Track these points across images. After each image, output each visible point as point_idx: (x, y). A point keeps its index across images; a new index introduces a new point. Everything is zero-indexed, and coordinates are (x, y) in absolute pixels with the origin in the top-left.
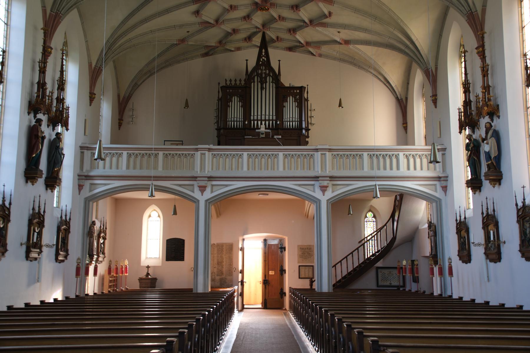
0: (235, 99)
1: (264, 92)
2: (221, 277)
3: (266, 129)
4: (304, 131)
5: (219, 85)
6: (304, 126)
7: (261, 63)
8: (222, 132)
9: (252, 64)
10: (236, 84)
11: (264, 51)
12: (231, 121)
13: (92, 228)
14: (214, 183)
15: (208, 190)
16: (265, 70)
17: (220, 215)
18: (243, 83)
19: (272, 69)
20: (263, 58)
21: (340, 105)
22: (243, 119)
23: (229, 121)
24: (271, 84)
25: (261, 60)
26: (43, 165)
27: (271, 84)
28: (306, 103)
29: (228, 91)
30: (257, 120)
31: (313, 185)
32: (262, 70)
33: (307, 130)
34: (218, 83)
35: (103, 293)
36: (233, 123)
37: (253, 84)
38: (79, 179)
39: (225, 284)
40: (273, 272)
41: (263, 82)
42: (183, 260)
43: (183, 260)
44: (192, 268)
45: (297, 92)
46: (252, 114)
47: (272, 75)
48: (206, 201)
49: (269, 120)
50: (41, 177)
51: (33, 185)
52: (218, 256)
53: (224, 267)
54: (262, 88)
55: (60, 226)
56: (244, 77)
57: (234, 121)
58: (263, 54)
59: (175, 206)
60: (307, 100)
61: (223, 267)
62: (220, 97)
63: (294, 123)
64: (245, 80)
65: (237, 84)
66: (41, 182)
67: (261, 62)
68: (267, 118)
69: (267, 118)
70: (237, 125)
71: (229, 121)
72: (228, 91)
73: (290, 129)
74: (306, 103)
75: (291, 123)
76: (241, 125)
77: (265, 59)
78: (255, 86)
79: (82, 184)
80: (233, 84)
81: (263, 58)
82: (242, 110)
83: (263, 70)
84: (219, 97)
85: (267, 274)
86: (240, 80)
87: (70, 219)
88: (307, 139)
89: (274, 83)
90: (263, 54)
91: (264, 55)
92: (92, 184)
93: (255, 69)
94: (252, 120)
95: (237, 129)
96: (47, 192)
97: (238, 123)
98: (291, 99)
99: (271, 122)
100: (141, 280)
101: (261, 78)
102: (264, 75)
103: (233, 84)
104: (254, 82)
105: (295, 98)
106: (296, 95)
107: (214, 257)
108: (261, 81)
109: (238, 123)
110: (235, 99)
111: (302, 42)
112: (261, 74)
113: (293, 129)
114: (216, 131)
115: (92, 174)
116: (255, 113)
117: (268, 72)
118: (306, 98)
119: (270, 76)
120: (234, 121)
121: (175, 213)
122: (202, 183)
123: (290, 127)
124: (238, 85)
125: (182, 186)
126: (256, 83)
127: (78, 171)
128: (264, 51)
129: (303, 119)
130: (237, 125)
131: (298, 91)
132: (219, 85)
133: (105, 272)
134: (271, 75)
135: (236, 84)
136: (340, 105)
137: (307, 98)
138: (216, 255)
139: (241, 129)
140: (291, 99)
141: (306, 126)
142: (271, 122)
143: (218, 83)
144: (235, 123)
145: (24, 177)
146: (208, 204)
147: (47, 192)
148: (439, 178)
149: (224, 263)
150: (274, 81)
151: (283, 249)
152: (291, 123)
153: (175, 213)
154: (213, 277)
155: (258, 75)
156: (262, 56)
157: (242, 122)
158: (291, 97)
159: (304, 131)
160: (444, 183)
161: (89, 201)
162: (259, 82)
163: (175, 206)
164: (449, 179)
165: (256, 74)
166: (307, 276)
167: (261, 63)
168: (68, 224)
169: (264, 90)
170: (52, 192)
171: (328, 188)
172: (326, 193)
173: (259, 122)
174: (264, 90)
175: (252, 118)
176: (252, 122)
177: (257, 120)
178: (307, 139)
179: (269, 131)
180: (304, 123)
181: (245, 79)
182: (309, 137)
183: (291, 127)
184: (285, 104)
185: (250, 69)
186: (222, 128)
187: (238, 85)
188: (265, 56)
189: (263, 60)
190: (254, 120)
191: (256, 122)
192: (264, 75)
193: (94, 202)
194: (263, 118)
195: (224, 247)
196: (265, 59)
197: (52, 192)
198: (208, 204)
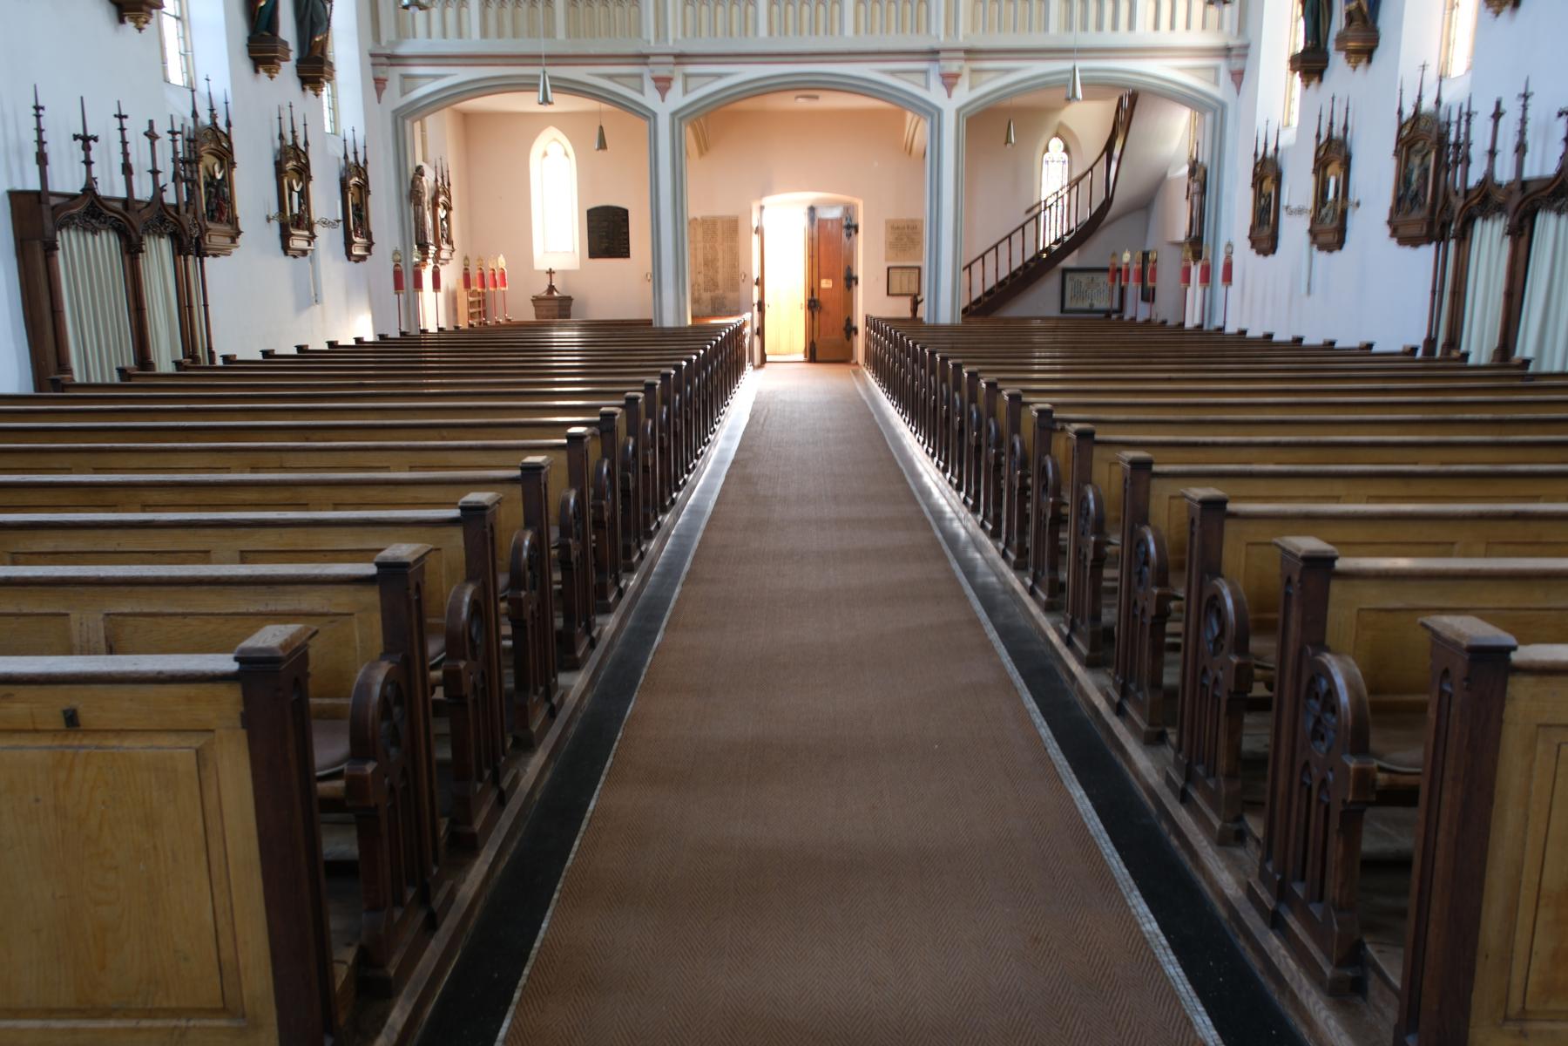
2: (712, 294)
13: (418, 182)
14: (690, 69)
15: (677, 86)
17: (707, 149)
26: (287, 28)
31: (925, 72)
35: (457, 328)
38: (373, 65)
39: (723, 309)
40: (830, 282)
42: (628, 257)
43: (628, 257)
44: (649, 276)
48: (674, 114)
50: (287, 60)
51: (271, 77)
52: (705, 248)
53: (720, 270)
55: (346, 176)
59: (601, 128)
61: (717, 272)
66: (288, 69)
79: (381, 76)
85: (815, 287)
87: (365, 161)
92: (405, 77)
96: (305, 97)
100: (537, 300)
107: (696, 249)
115: (404, 49)
121: (602, 145)
122: (662, 71)
125: (617, 79)
127: (369, 45)
133: (458, 283)
138: (700, 245)
145: (248, 59)
146: (677, 122)
147: (305, 97)
148: (1226, 51)
149: (720, 264)
151: (852, 228)
153: (602, 145)
154: (696, 294)
160: (1237, 64)
161: (404, 118)
163: (601, 128)
164: (1251, 52)
166: (905, 291)
168: (362, 172)
170: (317, 95)
171: (960, 80)
172: (956, 92)
193: (416, 121)
195: (719, 226)
197: (317, 95)
198: (677, 122)
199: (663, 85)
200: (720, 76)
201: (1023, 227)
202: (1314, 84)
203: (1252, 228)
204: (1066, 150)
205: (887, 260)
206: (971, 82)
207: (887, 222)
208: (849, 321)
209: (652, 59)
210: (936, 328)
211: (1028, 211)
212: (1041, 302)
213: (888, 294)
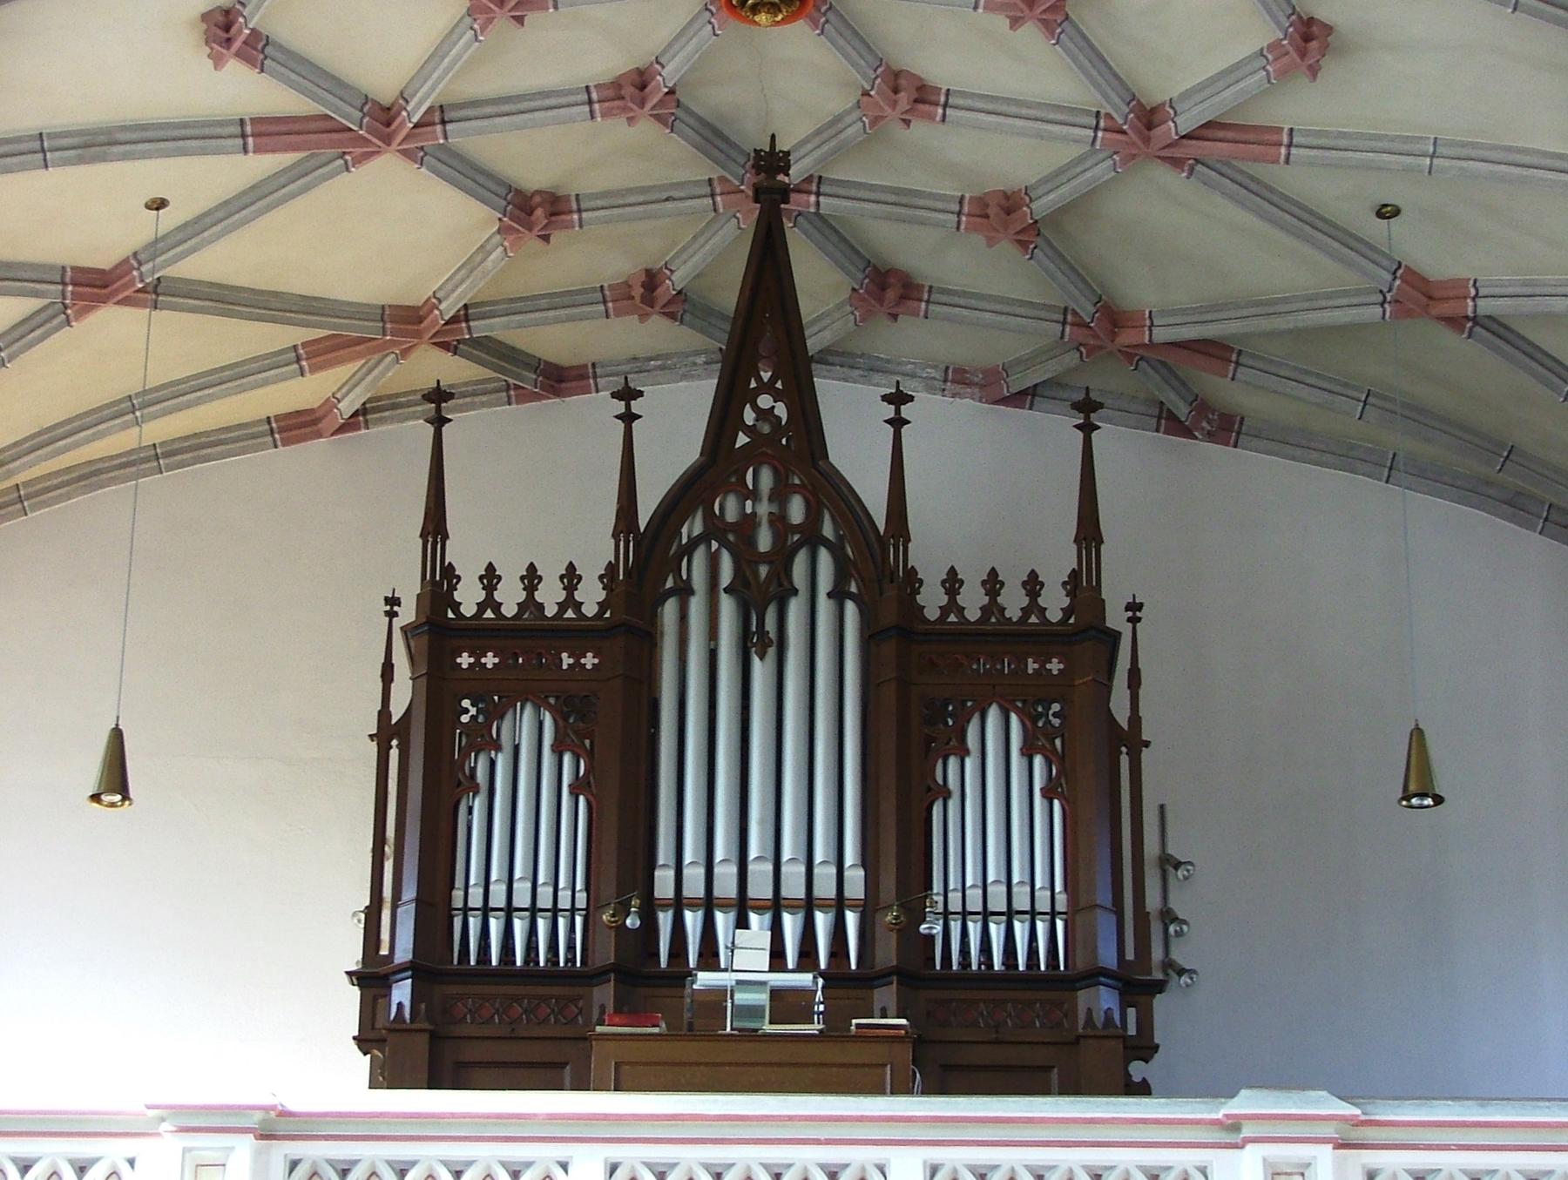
1: (761, 671)
5: (391, 615)
7: (742, 439)
8: (400, 1005)
12: (486, 910)
16: (780, 495)
18: (591, 596)
20: (765, 401)
22: (587, 888)
23: (466, 910)
24: (824, 607)
25: (749, 416)
27: (824, 607)
28: (1124, 760)
29: (465, 660)
34: (388, 601)
36: (495, 926)
37: (670, 609)
45: (1042, 672)
47: (840, 538)
62: (397, 712)
63: (1021, 930)
65: (541, 607)
67: (750, 431)
70: (531, 946)
71: (466, 910)
72: (465, 660)
73: (987, 978)
74: (1124, 760)
75: (996, 932)
76: (571, 947)
77: (781, 410)
80: (509, 610)
81: (765, 401)
82: (575, 816)
84: (384, 713)
86: (571, 578)
89: (852, 596)
91: (773, 380)
94: (665, 905)
95: (530, 974)
97: (542, 925)
99: (822, 921)
101: (745, 557)
102: (764, 541)
103: (509, 610)
104: (684, 591)
105: (1029, 720)
106: (1039, 701)
108: (747, 585)
109: (542, 925)
112: (748, 524)
117: (797, 511)
118: (1125, 725)
119: (812, 538)
120: (510, 910)
123: (990, 966)
124: (550, 611)
126: (696, 606)
130: (531, 946)
131: (1055, 666)
132: (391, 615)
134: (828, 530)
135: (530, 604)
137: (1135, 719)
139: (569, 977)
141: (1130, 955)
142: (822, 921)
143: (388, 601)
144: (519, 926)
150: (853, 589)
152: (996, 932)
155: (715, 529)
156: (753, 384)
157: (579, 920)
158: (993, 715)
159: (1105, 999)
162: (726, 590)
165: (698, 529)
167: (742, 439)
169: (772, 652)
173: (722, 920)
174: (772, 652)
175: (664, 883)
176: (665, 920)
181: (611, 568)
182: (1156, 1048)
183: (997, 965)
186: (402, 968)
187: (550, 611)
188: (779, 385)
189: (765, 415)
190: (679, 903)
192: (764, 541)
196: (781, 410)
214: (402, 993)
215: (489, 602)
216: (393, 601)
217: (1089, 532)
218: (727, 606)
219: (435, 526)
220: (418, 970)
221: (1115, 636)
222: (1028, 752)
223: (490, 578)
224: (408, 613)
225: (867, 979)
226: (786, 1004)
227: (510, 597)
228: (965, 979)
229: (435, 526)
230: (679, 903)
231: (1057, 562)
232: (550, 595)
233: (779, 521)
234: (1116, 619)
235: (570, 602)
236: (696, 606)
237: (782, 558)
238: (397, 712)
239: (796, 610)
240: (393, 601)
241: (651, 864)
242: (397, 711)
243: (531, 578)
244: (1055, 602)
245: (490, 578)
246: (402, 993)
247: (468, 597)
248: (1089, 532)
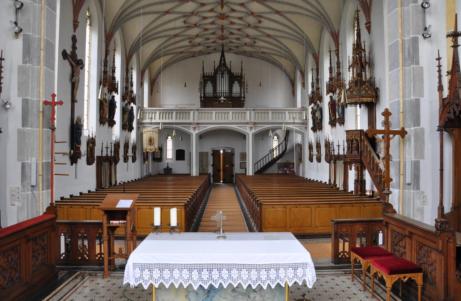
0: (209, 83)
1: (223, 79)
3: (224, 98)
4: (242, 99)
6: (242, 96)
9: (217, 64)
10: (209, 75)
11: (223, 58)
14: (200, 126)
15: (197, 129)
16: (224, 68)
18: (213, 74)
19: (226, 67)
21: (260, 85)
24: (226, 75)
27: (226, 75)
30: (220, 93)
32: (222, 68)
33: (244, 98)
37: (217, 75)
41: (223, 74)
46: (217, 90)
48: (196, 134)
49: (225, 93)
54: (222, 77)
56: (213, 71)
57: (208, 93)
58: (223, 60)
60: (244, 83)
61: (203, 163)
64: (214, 73)
68: (225, 92)
69: (225, 92)
75: (236, 95)
78: (219, 76)
79: (139, 126)
83: (223, 68)
88: (244, 102)
90: (223, 60)
92: (143, 126)
93: (218, 67)
98: (236, 82)
99: (226, 94)
101: (222, 72)
104: (218, 74)
105: (238, 82)
110: (209, 83)
111: (242, 51)
113: (237, 97)
114: (200, 98)
116: (219, 89)
117: (225, 69)
119: (226, 71)
120: (208, 93)
122: (194, 126)
126: (219, 75)
128: (223, 58)
129: (242, 92)
135: (209, 75)
136: (260, 85)
139: (212, 97)
140: (236, 82)
142: (226, 94)
148: (303, 124)
149: (204, 162)
152: (236, 95)
159: (242, 99)
160: (305, 126)
164: (308, 123)
172: (252, 130)
175: (217, 92)
176: (217, 94)
177: (220, 93)
178: (244, 102)
179: (225, 99)
180: (242, 94)
184: (234, 85)
185: (216, 69)
190: (218, 93)
191: (219, 94)
192: (223, 71)
194: (223, 92)
199: (195, 128)
200: (206, 127)
201: (268, 154)
202: (315, 133)
203: (309, 157)
204: (278, 138)
205: (240, 161)
206: (255, 128)
207: (240, 153)
208: (232, 174)
209: (192, 124)
210: (249, 176)
211: (270, 151)
212: (274, 169)
213: (241, 168)
214: (203, 99)
215: (207, 75)
216: (201, 74)
217: (242, 70)
218: (221, 75)
219: (203, 70)
220: (204, 97)
221: (243, 77)
222: (238, 84)
223: (207, 73)
224: (202, 76)
225: (229, 97)
226: (224, 101)
227: (208, 74)
228: (234, 97)
229: (203, 70)
230: (218, 93)
231: (240, 72)
232: (210, 74)
233: (224, 69)
234: (243, 76)
235: (211, 75)
236: (219, 75)
237: (224, 72)
238: (201, 81)
239: (225, 75)
240: (201, 74)
241: (216, 91)
242: (201, 81)
243: (209, 73)
244: (240, 74)
245: (207, 73)
246: (203, 99)
247: (205, 74)
248: (242, 70)
